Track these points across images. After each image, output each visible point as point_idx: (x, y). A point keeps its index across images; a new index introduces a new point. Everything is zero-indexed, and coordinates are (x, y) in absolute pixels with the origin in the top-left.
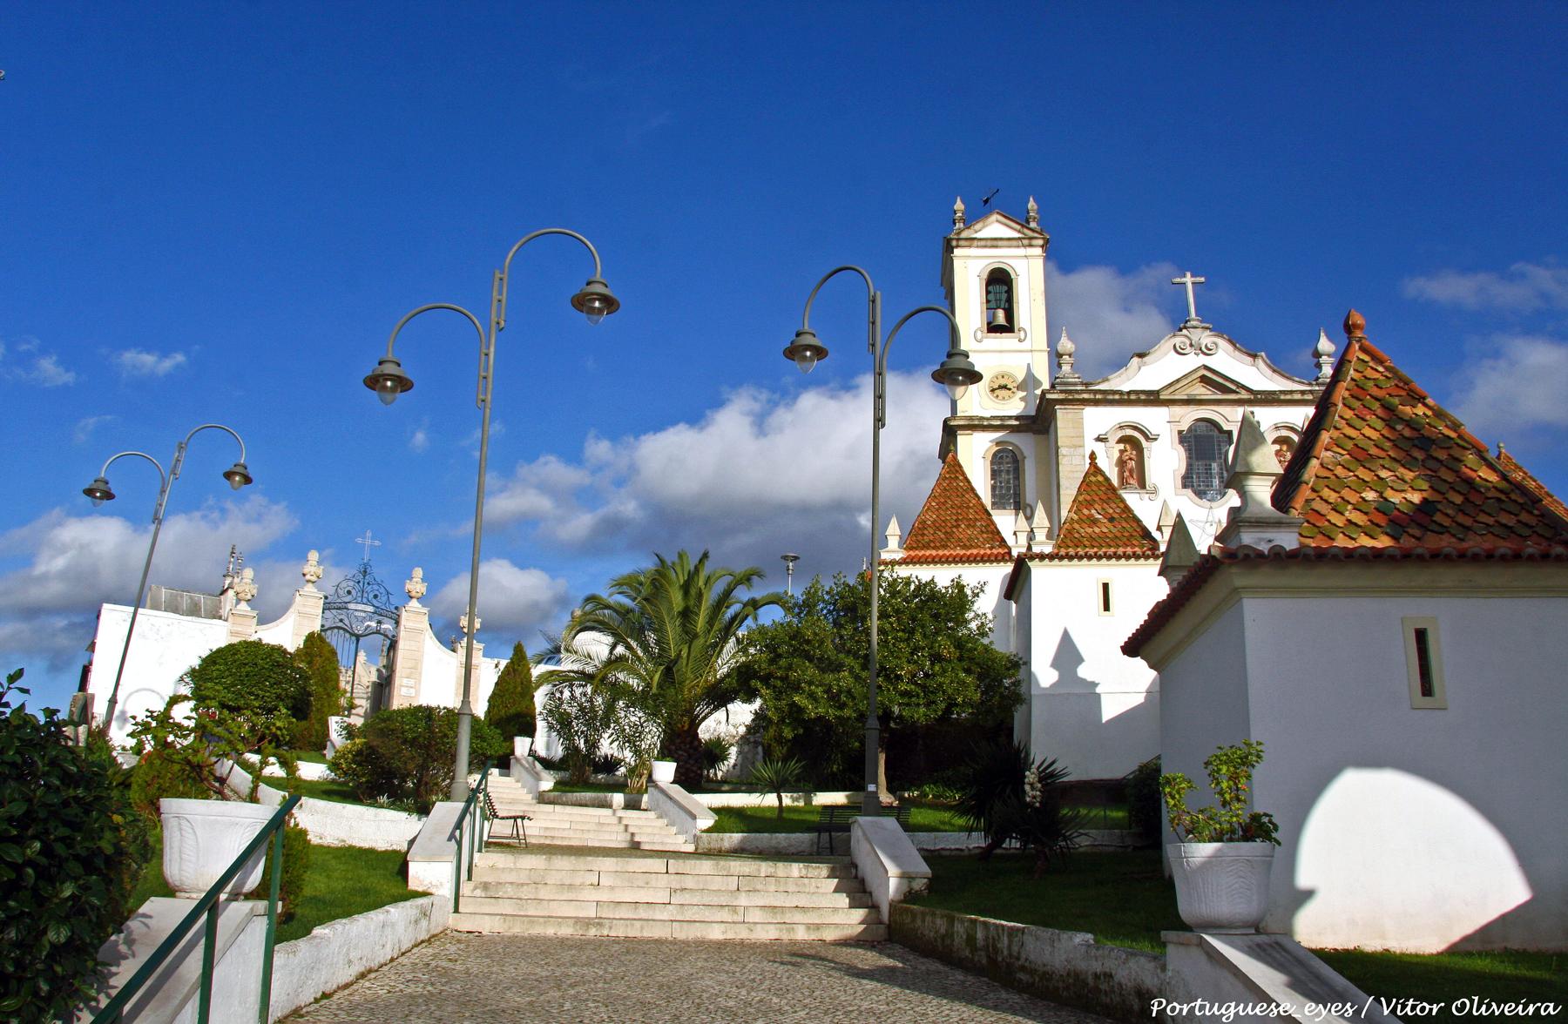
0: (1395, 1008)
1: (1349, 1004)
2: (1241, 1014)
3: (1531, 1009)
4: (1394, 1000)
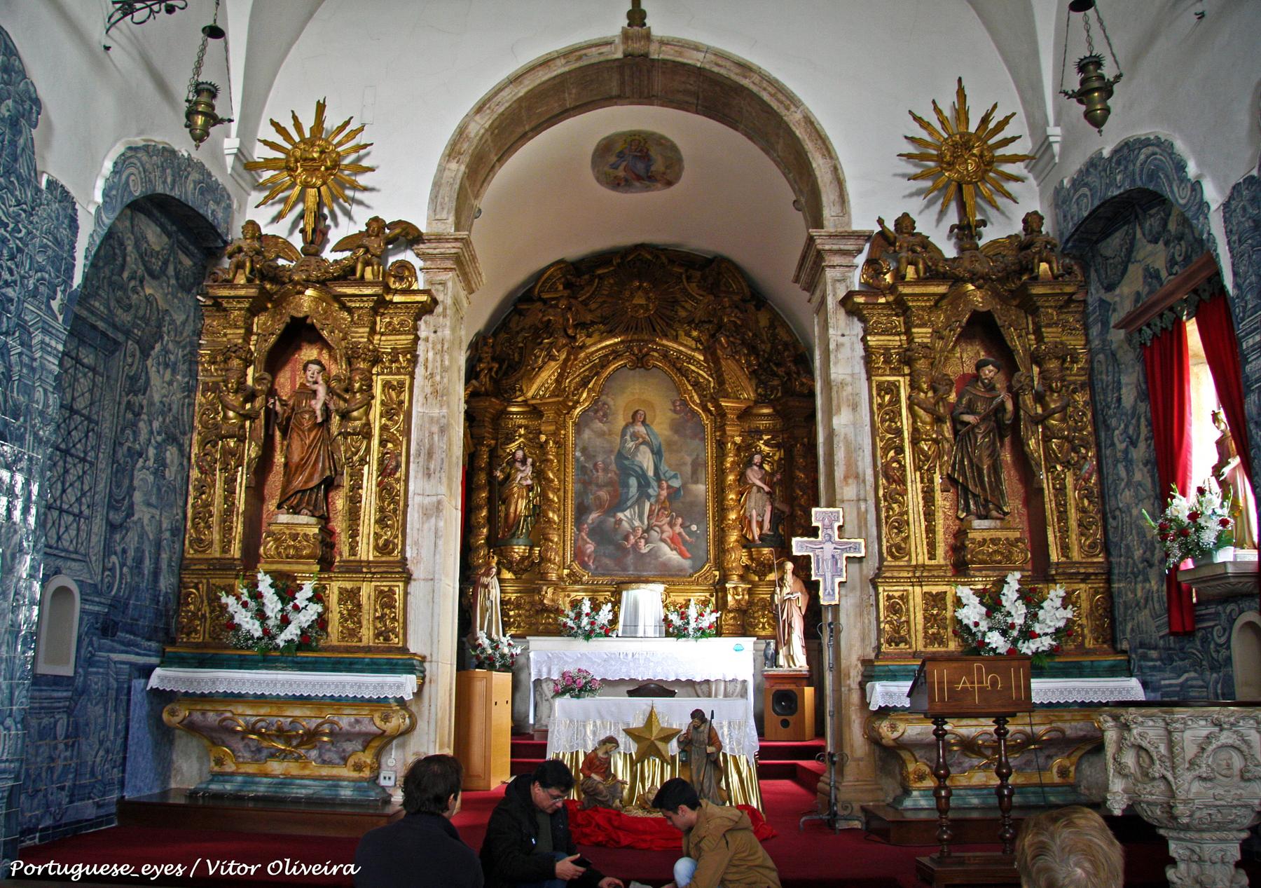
0: (219, 868)
1: (180, 865)
2: (88, 873)
3: (335, 869)
4: (218, 862)
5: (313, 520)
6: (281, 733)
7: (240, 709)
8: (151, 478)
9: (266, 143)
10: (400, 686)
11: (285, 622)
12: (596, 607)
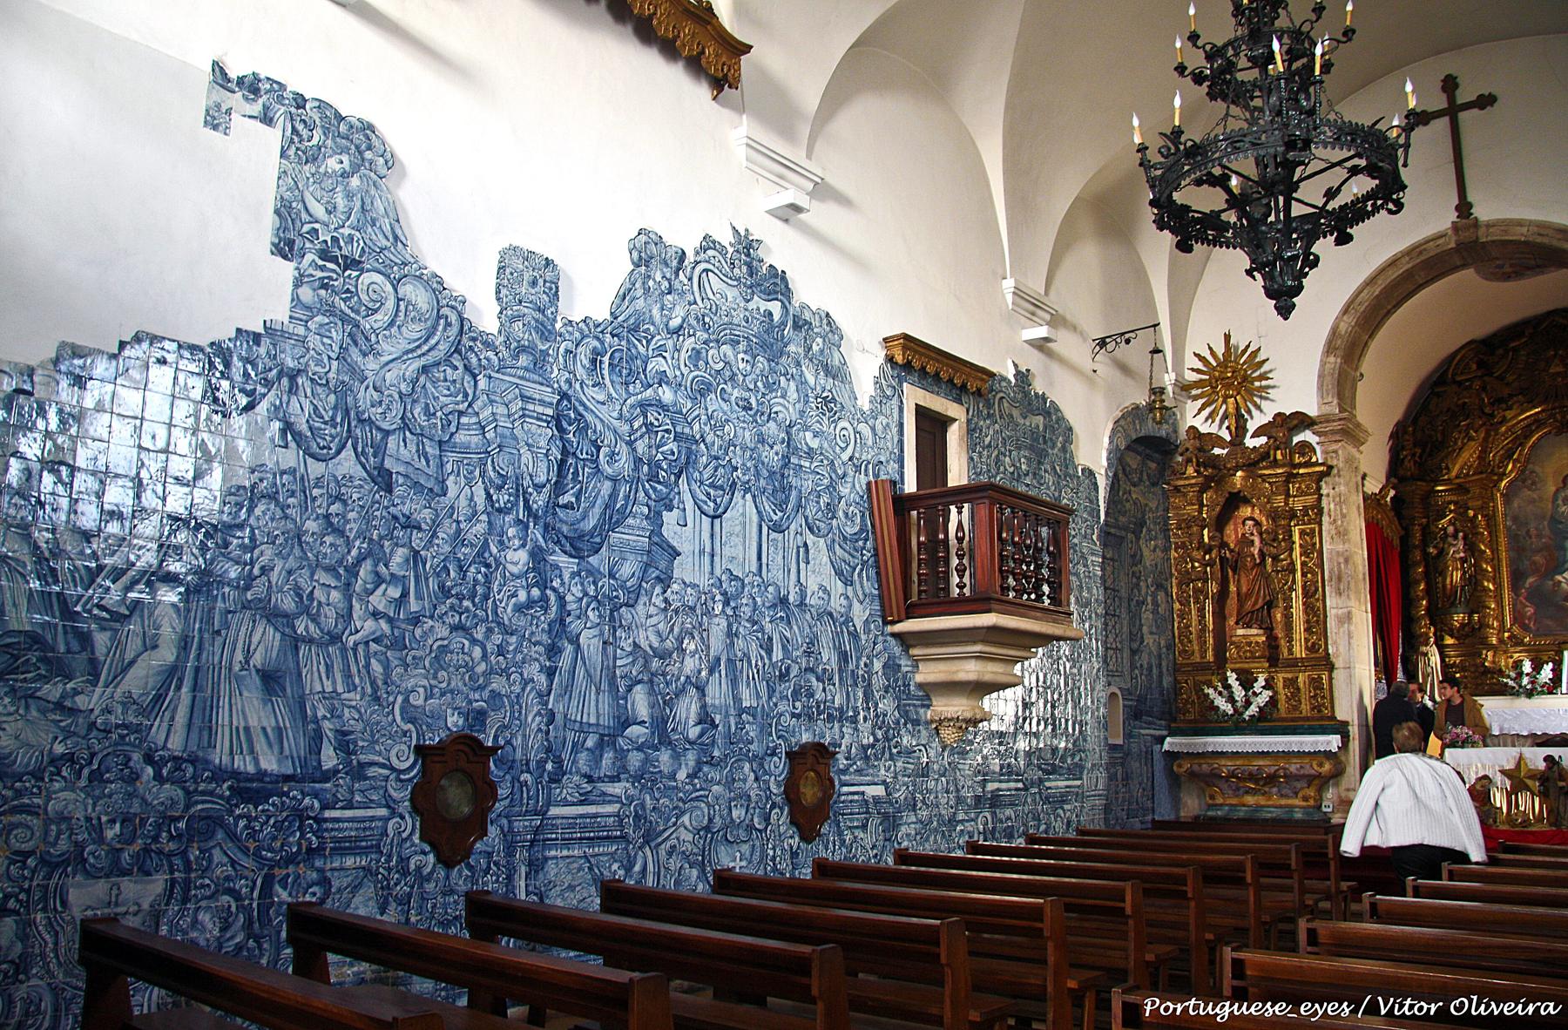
0: (1393, 1007)
2: (1236, 1013)
3: (1531, 1008)
5: (1261, 632)
6: (1252, 777)
7: (1223, 762)
8: (1151, 616)
9: (1193, 370)
10: (1328, 743)
11: (1248, 703)
12: (1537, 668)
